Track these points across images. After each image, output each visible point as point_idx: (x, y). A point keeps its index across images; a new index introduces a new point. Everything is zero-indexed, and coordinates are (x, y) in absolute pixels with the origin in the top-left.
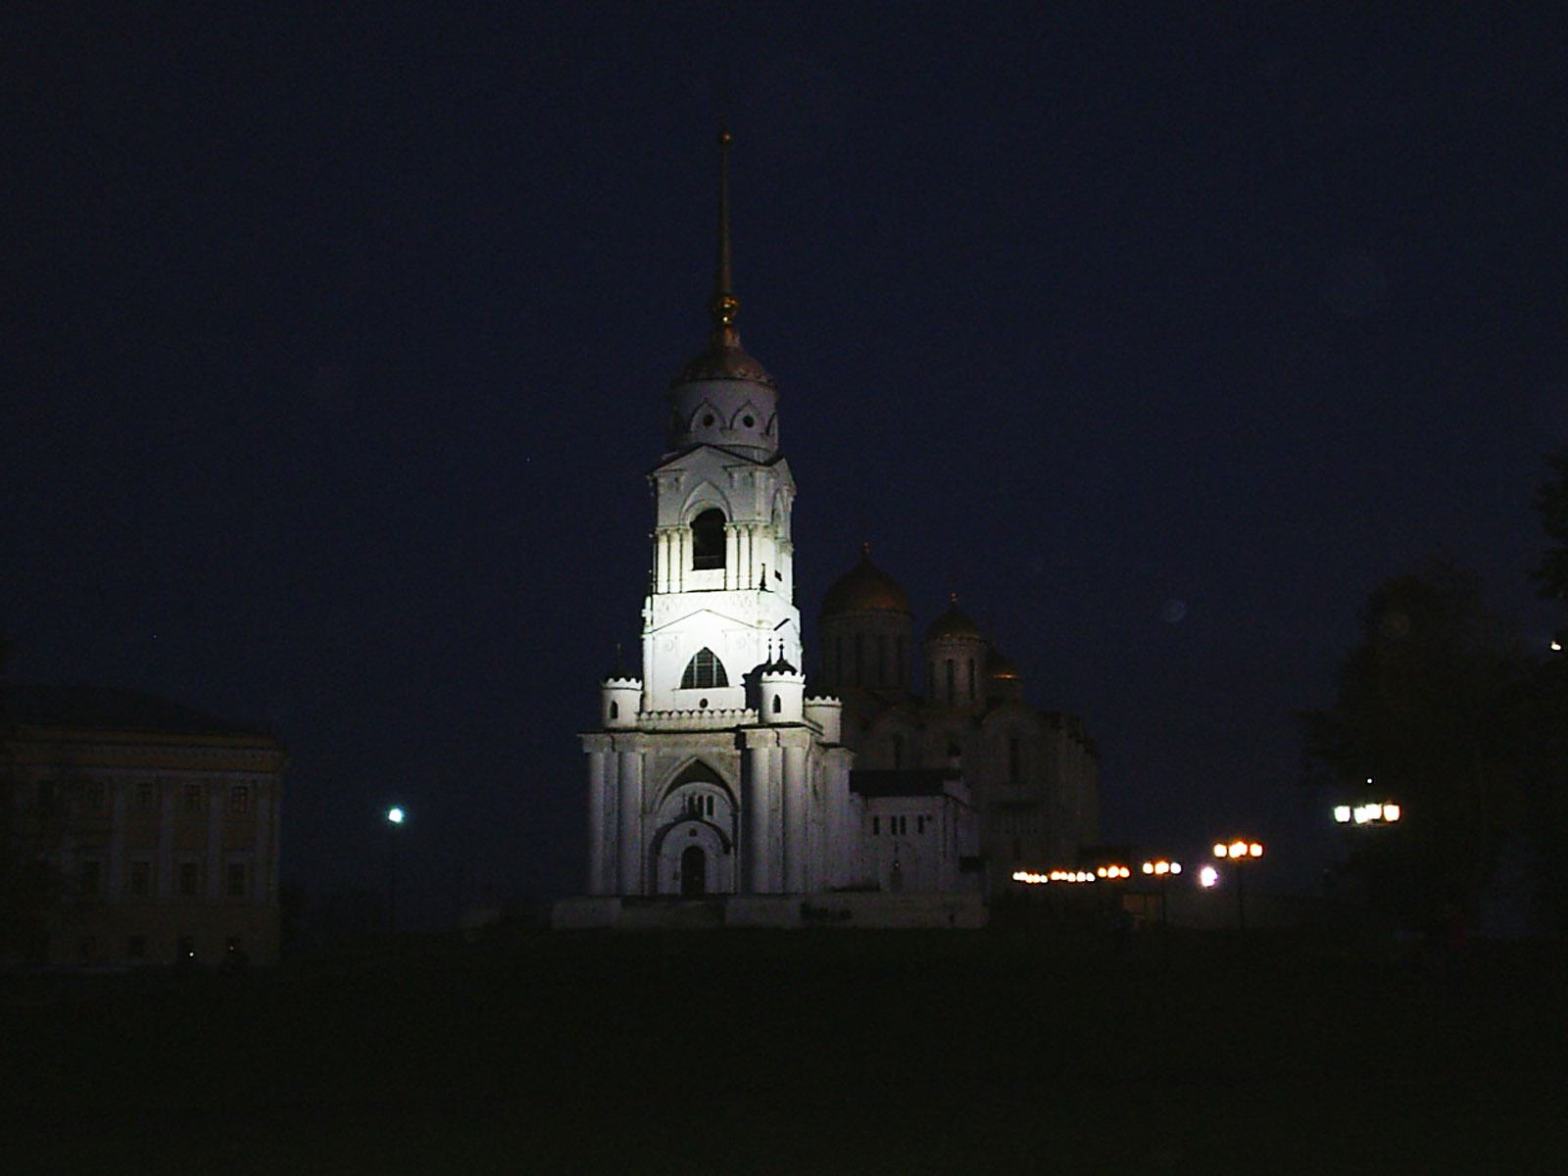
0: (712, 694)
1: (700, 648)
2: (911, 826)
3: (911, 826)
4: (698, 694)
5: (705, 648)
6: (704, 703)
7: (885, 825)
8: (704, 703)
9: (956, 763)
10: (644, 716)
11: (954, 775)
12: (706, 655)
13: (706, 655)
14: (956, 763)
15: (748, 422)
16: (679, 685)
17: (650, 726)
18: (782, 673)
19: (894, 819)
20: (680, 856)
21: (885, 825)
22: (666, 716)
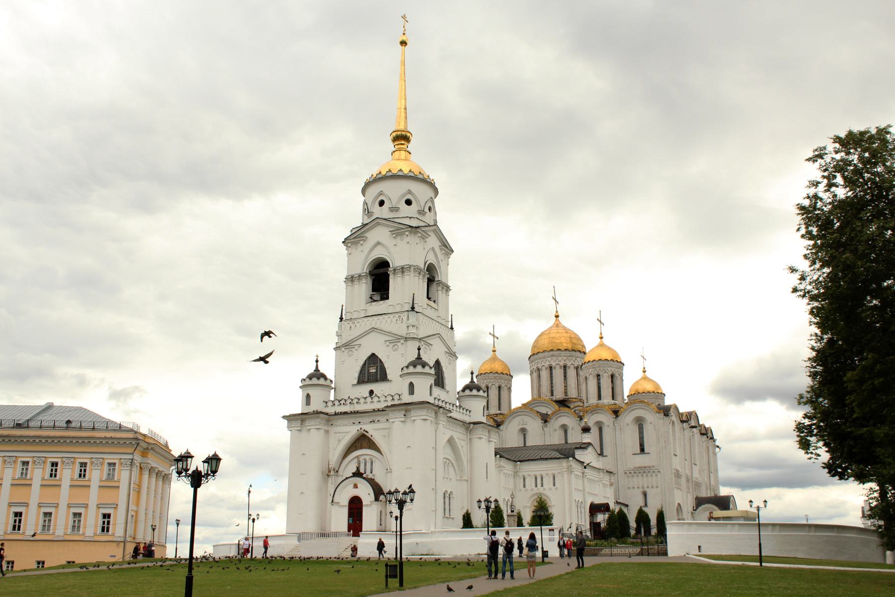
0: (378, 388)
1: (369, 354)
2: (548, 482)
3: (548, 482)
4: (367, 388)
5: (373, 355)
6: (371, 392)
7: (530, 482)
8: (371, 392)
9: (586, 438)
10: (330, 404)
11: (584, 446)
12: (373, 359)
13: (373, 359)
14: (586, 438)
15: (409, 202)
16: (356, 381)
17: (331, 410)
18: (415, 367)
19: (536, 479)
20: (347, 503)
21: (530, 482)
22: (342, 402)
